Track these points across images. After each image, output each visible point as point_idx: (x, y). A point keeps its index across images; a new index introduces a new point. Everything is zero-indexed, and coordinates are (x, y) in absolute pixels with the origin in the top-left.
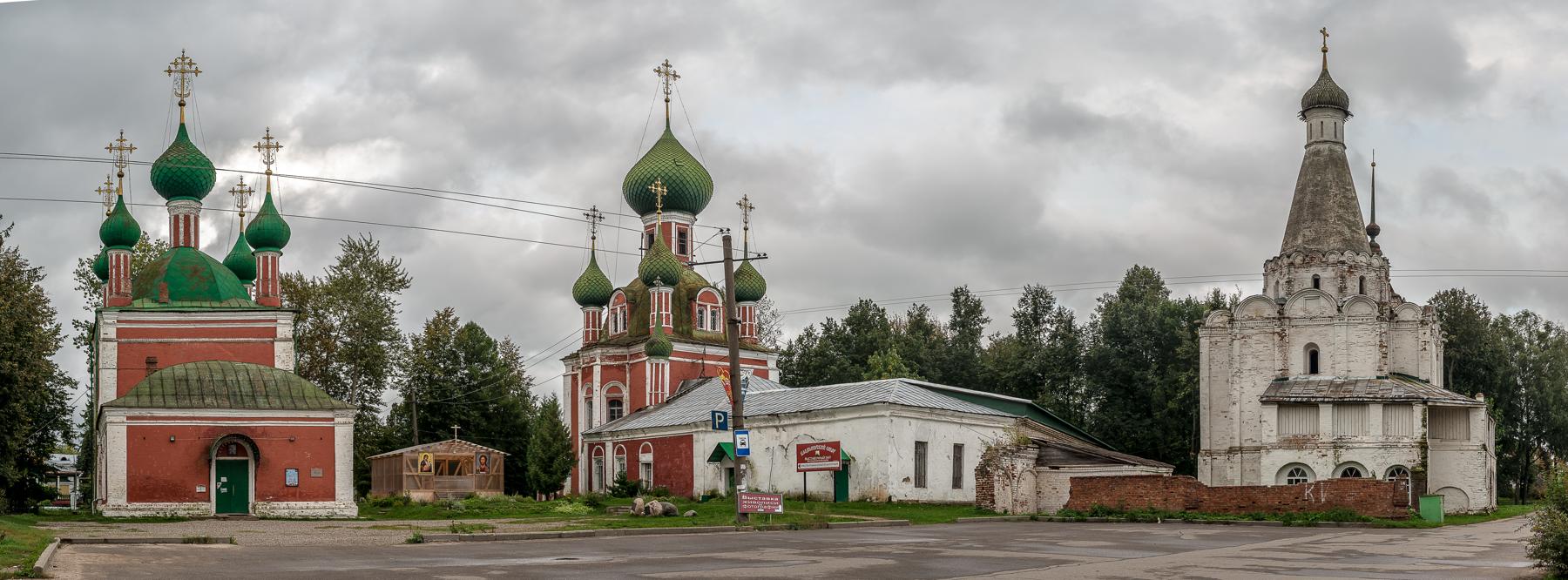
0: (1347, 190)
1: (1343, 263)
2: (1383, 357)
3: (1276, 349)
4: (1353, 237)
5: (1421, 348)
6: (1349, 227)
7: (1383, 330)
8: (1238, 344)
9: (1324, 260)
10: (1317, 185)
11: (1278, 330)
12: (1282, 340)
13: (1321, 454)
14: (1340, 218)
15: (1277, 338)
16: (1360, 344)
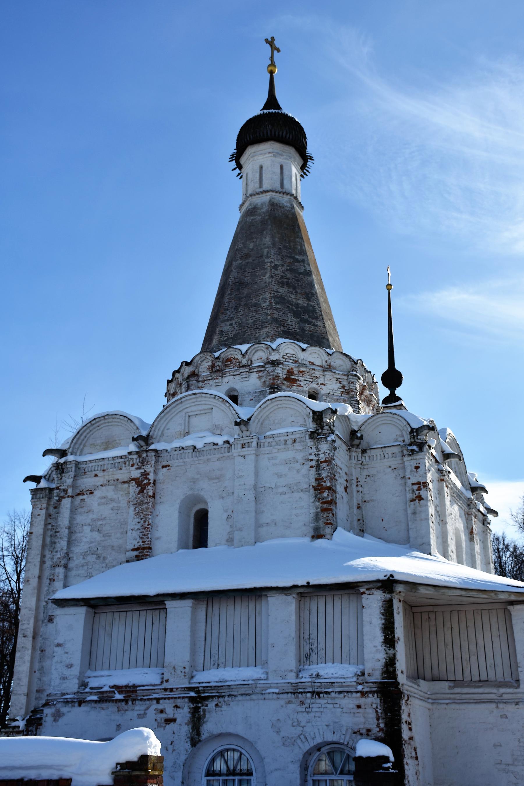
0: (298, 261)
1: (275, 363)
2: (323, 510)
3: (132, 508)
4: (302, 329)
5: (410, 496)
6: (296, 315)
7: (322, 458)
8: (69, 506)
9: (244, 362)
10: (247, 256)
11: (136, 474)
12: (141, 491)
13: (163, 716)
14: (281, 300)
15: (133, 489)
16: (281, 490)
